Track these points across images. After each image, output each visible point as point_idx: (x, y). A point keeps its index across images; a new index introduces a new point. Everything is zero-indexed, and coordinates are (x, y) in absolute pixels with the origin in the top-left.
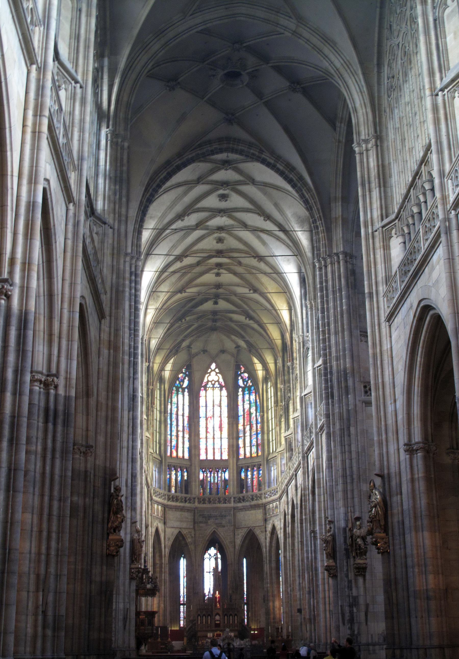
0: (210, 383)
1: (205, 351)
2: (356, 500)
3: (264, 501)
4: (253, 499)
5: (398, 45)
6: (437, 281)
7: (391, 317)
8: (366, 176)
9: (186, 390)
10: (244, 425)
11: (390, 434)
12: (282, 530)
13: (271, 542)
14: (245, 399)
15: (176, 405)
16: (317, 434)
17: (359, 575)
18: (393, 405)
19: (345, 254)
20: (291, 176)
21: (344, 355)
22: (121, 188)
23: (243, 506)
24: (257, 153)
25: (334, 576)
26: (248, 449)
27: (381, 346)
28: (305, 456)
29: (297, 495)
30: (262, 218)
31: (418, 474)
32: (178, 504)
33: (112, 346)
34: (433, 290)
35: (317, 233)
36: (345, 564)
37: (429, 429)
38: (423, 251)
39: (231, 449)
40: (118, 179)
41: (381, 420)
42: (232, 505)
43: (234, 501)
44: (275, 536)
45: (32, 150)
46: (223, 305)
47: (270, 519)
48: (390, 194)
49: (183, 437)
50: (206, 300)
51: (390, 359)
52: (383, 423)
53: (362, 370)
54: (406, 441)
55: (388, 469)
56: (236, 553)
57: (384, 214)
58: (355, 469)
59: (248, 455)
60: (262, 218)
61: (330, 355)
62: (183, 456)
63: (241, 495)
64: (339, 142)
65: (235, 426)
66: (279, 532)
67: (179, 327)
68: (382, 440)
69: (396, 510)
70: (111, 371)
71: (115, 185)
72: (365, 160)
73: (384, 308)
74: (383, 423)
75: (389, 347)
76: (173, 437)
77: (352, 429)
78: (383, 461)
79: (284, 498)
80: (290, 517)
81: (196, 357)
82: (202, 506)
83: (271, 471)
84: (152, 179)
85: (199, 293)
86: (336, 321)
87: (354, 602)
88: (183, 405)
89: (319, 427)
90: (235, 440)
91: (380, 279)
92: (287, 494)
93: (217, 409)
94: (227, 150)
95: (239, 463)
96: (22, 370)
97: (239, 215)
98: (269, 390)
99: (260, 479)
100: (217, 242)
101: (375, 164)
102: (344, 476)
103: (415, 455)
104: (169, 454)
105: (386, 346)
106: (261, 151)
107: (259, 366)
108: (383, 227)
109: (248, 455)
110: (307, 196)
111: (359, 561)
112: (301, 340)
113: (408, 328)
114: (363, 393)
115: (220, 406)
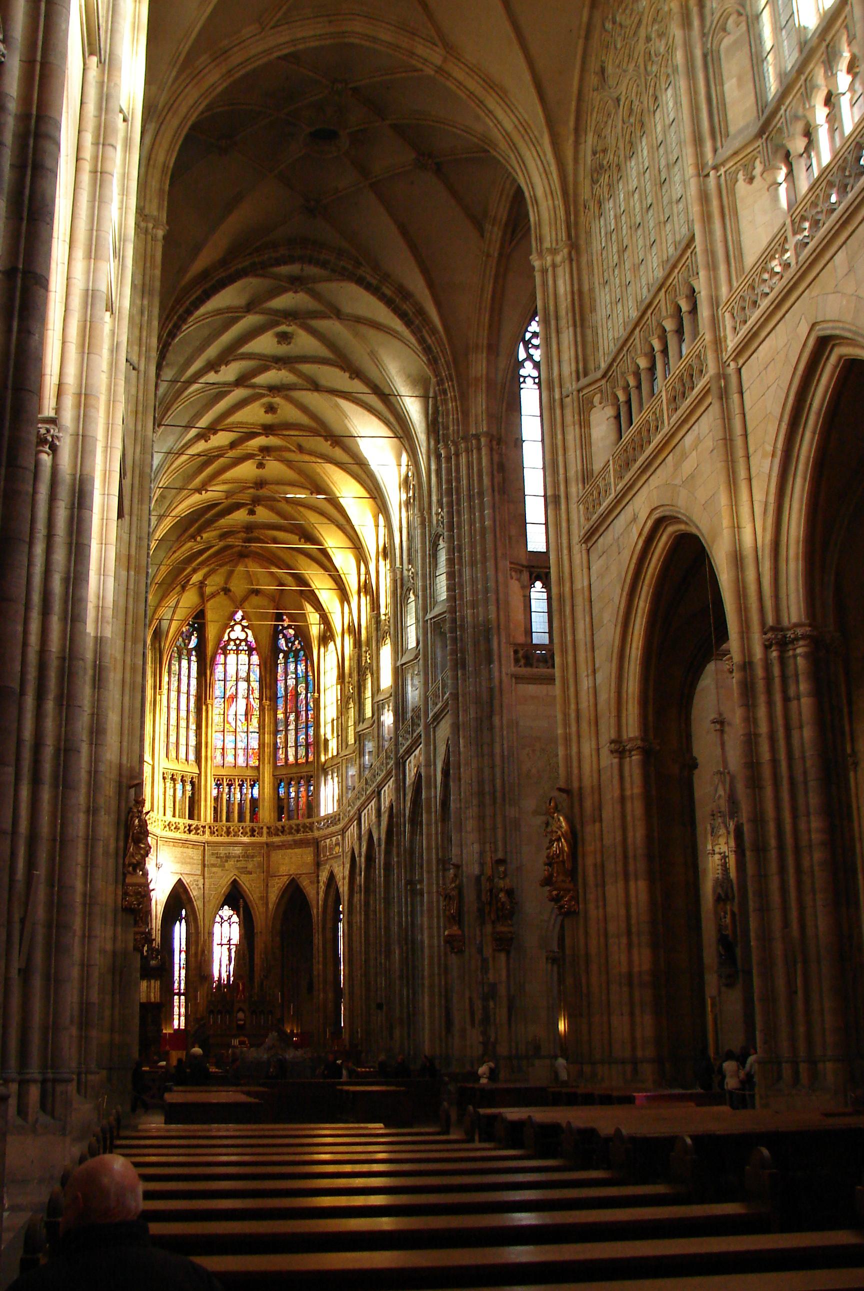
0: (232, 643)
1: (226, 591)
2: (500, 832)
3: (316, 834)
4: (298, 831)
5: (618, 100)
6: (692, 476)
7: (591, 536)
8: (552, 308)
9: (194, 653)
10: (285, 713)
11: (584, 726)
12: (347, 880)
13: (326, 900)
14: (289, 671)
16: (427, 726)
17: (500, 951)
18: (591, 678)
19: (491, 438)
20: (405, 306)
21: (486, 600)
22: (150, 305)
23: (282, 842)
24: (350, 267)
25: (460, 952)
26: (291, 752)
27: (572, 583)
28: (400, 764)
29: (379, 825)
30: (347, 375)
31: (632, 788)
32: (178, 835)
33: (133, 565)
34: (683, 492)
35: (445, 402)
36: (478, 933)
37: (650, 718)
38: (666, 429)
40: (147, 288)
41: (569, 703)
42: (264, 839)
43: (269, 834)
44: (332, 890)
45: (92, 200)
46: (263, 514)
47: (325, 864)
48: (590, 339)
49: (188, 727)
50: (237, 506)
51: (587, 603)
52: (573, 706)
53: (512, 625)
54: (613, 735)
55: (580, 779)
56: (269, 914)
57: (581, 370)
58: (498, 782)
59: (291, 759)
60: (347, 375)
61: (462, 598)
62: (187, 760)
63: (279, 824)
64: (488, 256)
66: (340, 884)
67: (191, 548)
68: (570, 734)
69: (590, 846)
70: (131, 607)
71: (143, 297)
72: (550, 282)
73: (579, 521)
74: (573, 706)
75: (586, 583)
76: (171, 728)
77: (496, 720)
78: (571, 767)
79: (353, 830)
80: (363, 859)
81: (212, 601)
82: (214, 839)
84: (178, 301)
85: (229, 494)
86: (473, 546)
87: (491, 993)
89: (430, 716)
91: (572, 473)
92: (359, 824)
93: (243, 685)
94: (301, 259)
96: (75, 578)
97: (306, 368)
99: (310, 798)
100: (266, 412)
101: (568, 289)
102: (481, 793)
103: (628, 759)
105: (580, 583)
106: (358, 264)
107: (313, 618)
108: (579, 391)
109: (291, 759)
110: (430, 341)
111: (500, 928)
112: (398, 576)
113: (626, 554)
114: (512, 661)
115: (248, 680)
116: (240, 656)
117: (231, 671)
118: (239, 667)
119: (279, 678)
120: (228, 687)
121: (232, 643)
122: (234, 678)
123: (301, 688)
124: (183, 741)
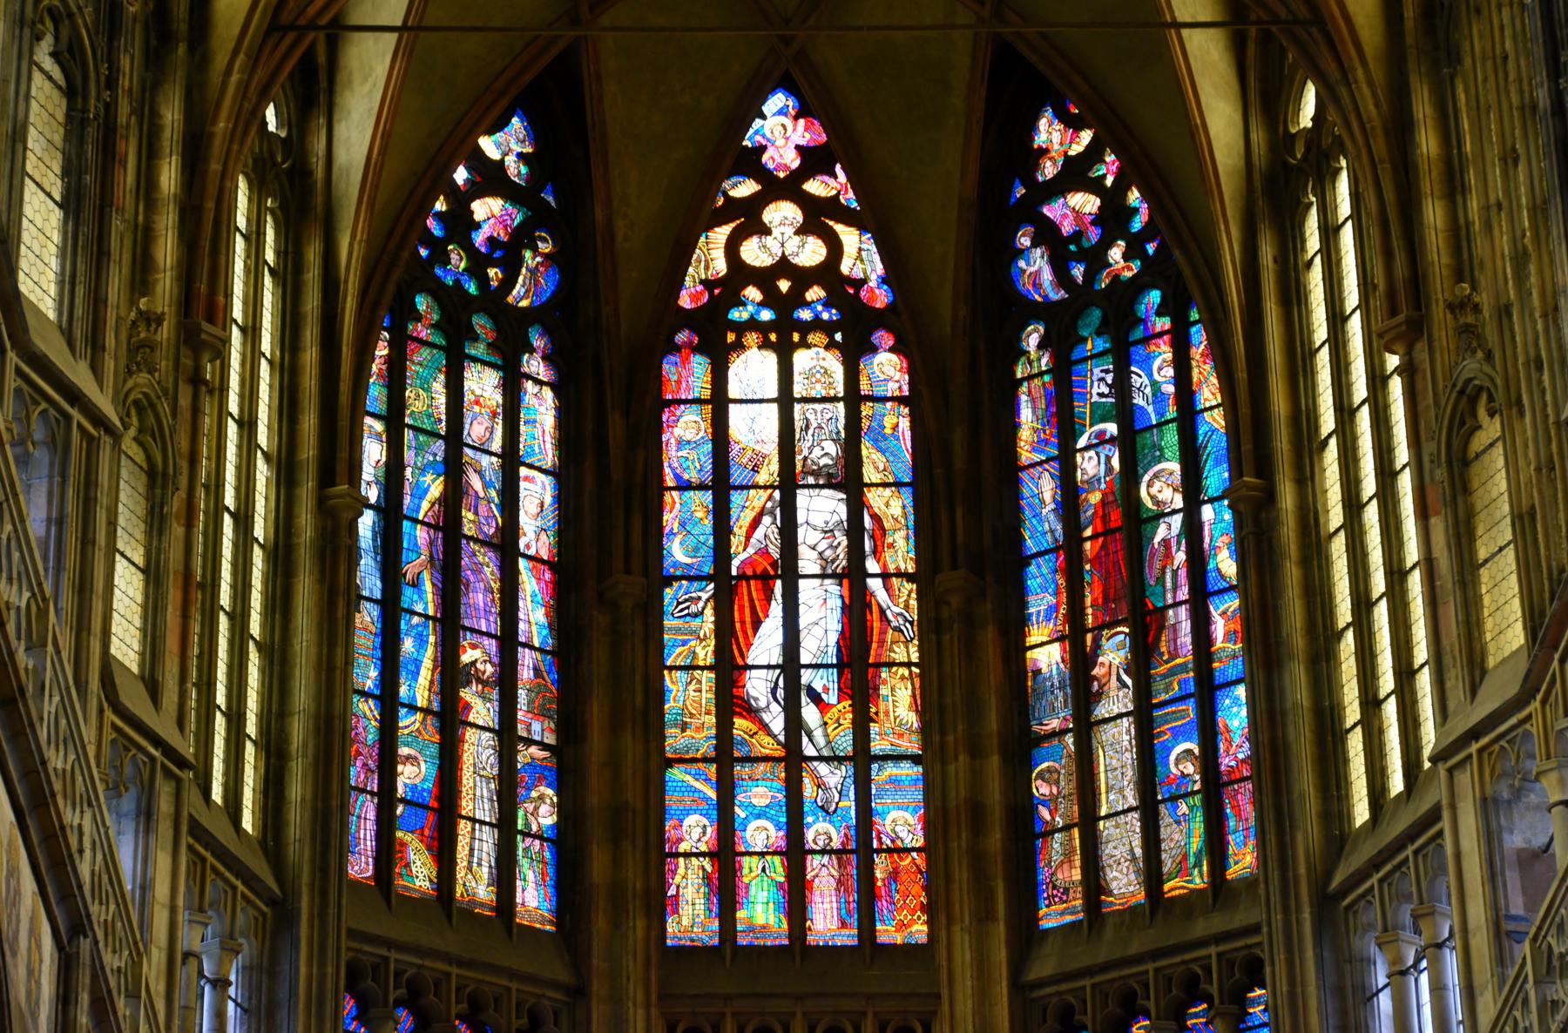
0: (753, 293)
9: (538, 342)
14: (1082, 409)
15: (439, 447)
26: (1121, 841)
39: (960, 842)
49: (506, 735)
59: (1123, 883)
65: (989, 637)
76: (408, 722)
83: (1371, 996)
88: (511, 459)
90: (994, 762)
93: (820, 509)
95: (1043, 967)
98: (1316, 279)
104: (361, 866)
109: (1123, 883)
116: (802, 360)
117: (754, 428)
118: (797, 407)
119: (1026, 455)
120: (741, 520)
121: (753, 293)
122: (770, 471)
123: (1161, 487)
124: (477, 797)
